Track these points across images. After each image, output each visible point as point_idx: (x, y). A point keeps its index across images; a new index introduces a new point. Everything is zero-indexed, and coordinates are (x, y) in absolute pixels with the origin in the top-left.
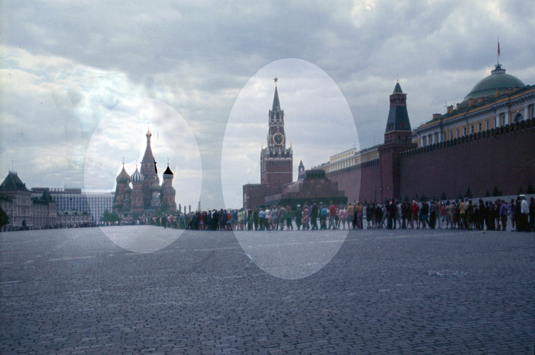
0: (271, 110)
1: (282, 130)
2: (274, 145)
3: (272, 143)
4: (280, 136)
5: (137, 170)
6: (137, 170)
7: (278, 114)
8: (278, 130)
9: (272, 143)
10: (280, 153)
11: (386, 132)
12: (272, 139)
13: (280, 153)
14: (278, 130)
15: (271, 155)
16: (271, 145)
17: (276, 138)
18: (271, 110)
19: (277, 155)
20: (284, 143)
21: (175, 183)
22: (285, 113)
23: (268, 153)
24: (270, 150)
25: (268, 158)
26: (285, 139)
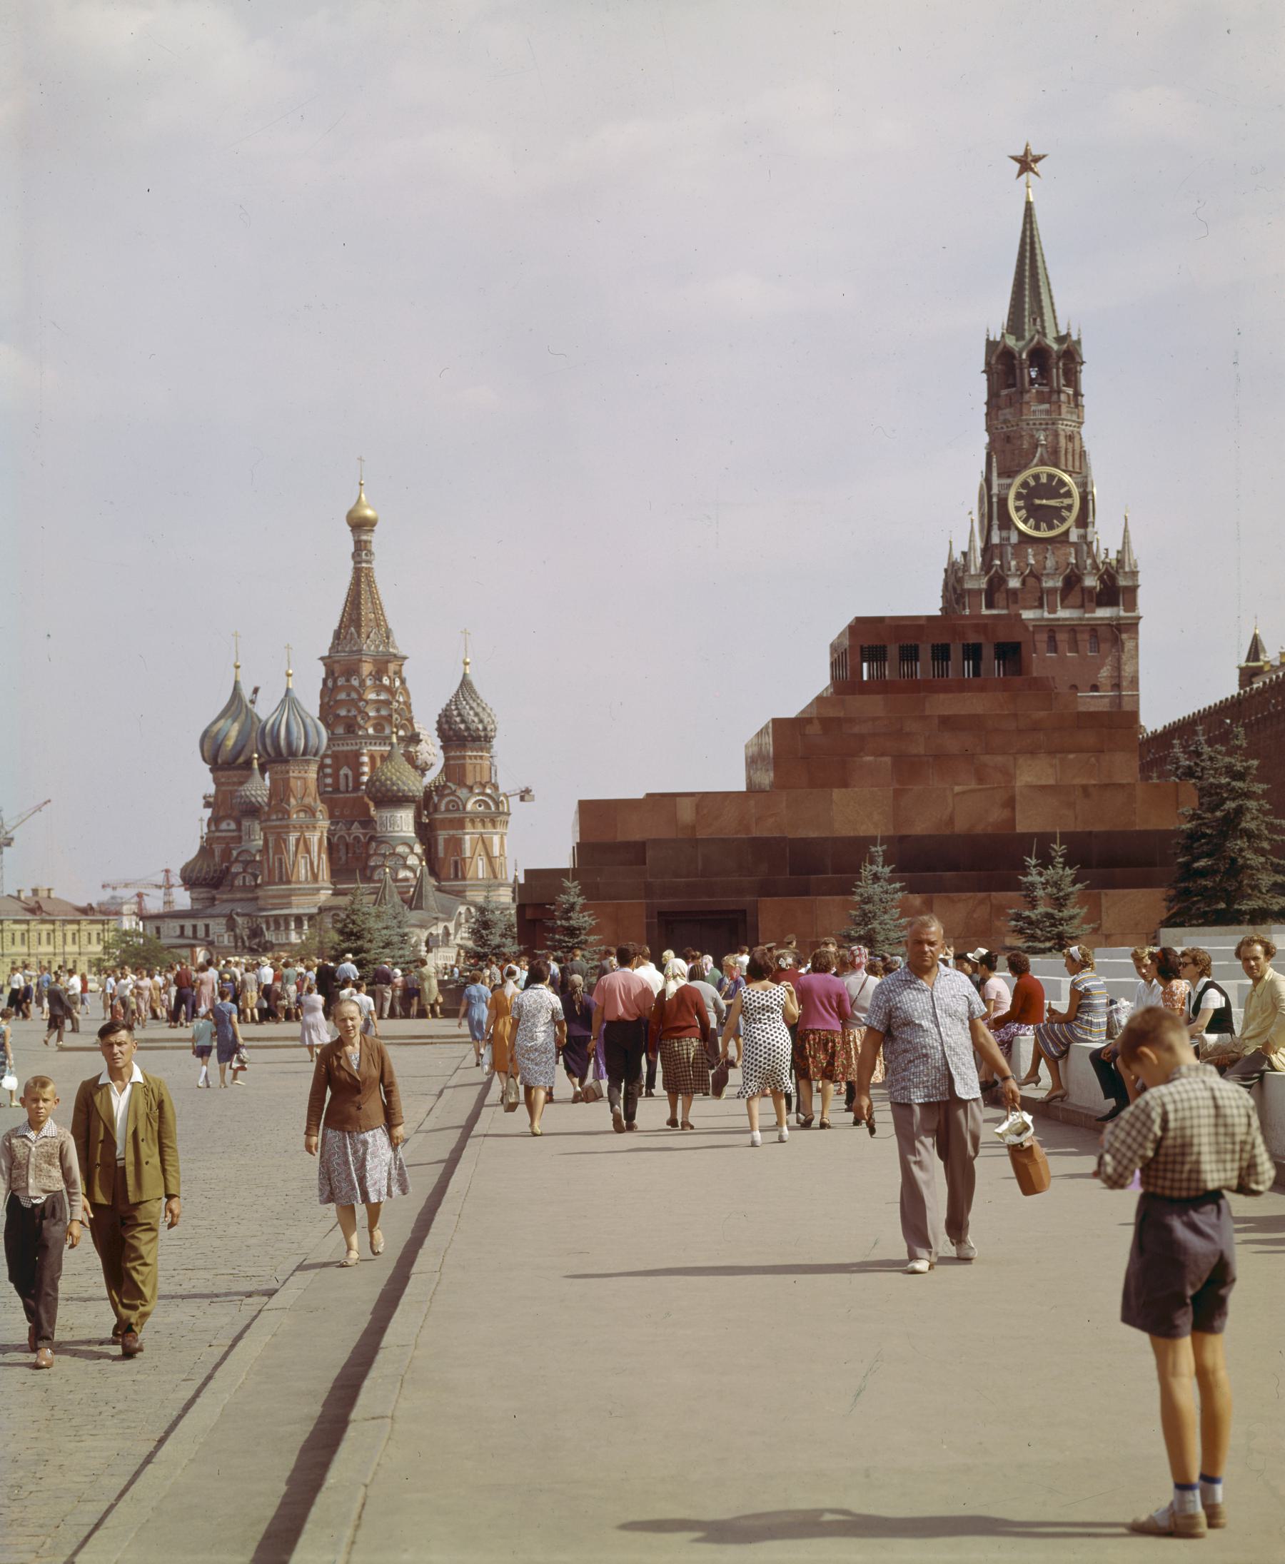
2: (1014, 538)
3: (1006, 523)
4: (1054, 488)
7: (1039, 355)
12: (1003, 502)
17: (1029, 495)
20: (1083, 520)
22: (1086, 352)
26: (1085, 498)
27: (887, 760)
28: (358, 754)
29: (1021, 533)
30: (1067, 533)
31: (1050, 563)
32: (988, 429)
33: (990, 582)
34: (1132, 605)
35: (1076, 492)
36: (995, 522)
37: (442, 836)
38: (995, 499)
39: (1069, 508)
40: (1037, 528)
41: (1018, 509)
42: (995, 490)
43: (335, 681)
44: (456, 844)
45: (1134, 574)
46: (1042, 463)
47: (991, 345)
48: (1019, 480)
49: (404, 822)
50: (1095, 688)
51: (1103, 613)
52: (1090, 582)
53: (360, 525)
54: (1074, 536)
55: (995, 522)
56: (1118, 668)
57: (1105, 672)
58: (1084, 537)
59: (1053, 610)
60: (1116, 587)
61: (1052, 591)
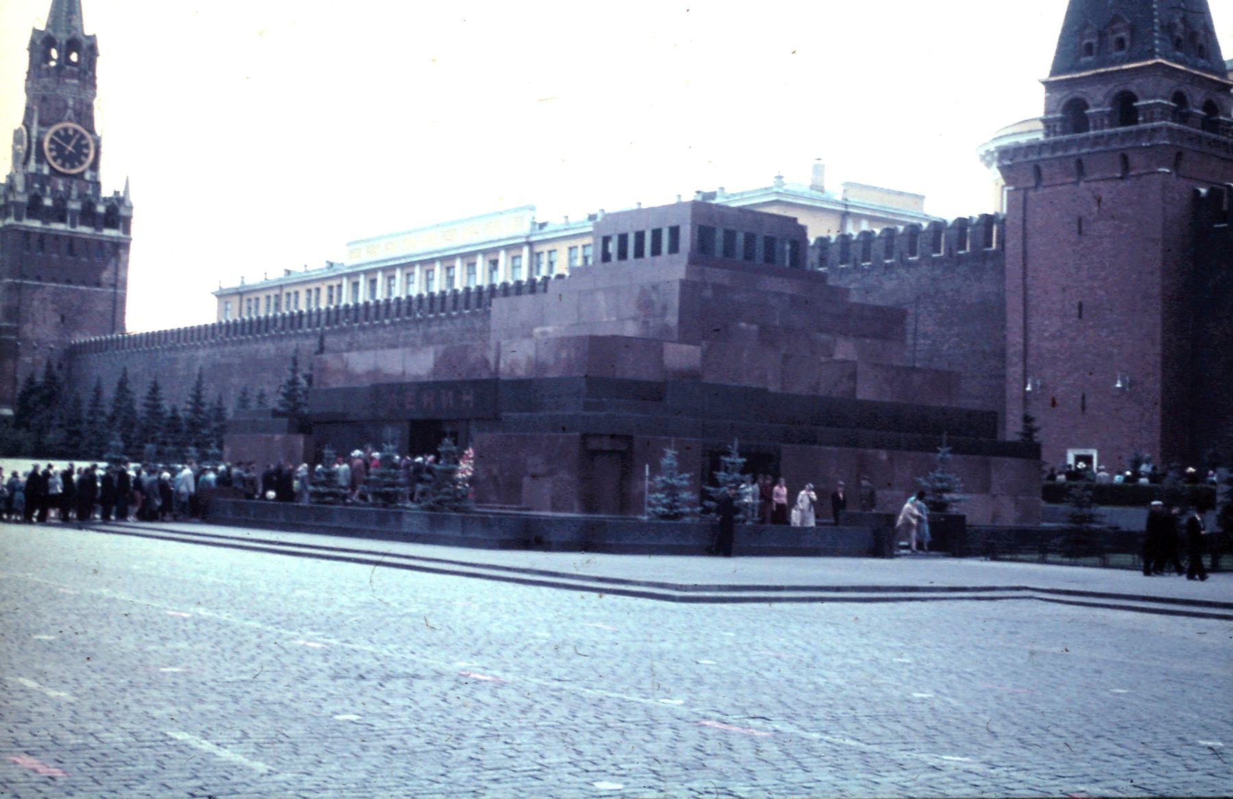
0: (42, 27)
1: (85, 115)
2: (46, 171)
3: (41, 158)
7: (73, 44)
8: (70, 112)
9: (41, 158)
11: (1053, 73)
12: (40, 144)
13: (75, 206)
14: (70, 112)
15: (34, 208)
16: (32, 166)
19: (59, 213)
20: (95, 166)
24: (28, 186)
25: (19, 218)
27: (754, 327)
29: (52, 168)
30: (82, 173)
31: (74, 193)
34: (127, 230)
35: (92, 146)
36: (33, 157)
38: (34, 140)
39: (87, 155)
40: (63, 165)
41: (51, 150)
42: (34, 133)
45: (131, 208)
46: (70, 120)
47: (35, 31)
48: (52, 130)
50: (98, 284)
51: (108, 232)
54: (88, 176)
55: (33, 157)
56: (116, 274)
57: (106, 275)
58: (95, 177)
59: (73, 225)
60: (116, 214)
61: (73, 212)
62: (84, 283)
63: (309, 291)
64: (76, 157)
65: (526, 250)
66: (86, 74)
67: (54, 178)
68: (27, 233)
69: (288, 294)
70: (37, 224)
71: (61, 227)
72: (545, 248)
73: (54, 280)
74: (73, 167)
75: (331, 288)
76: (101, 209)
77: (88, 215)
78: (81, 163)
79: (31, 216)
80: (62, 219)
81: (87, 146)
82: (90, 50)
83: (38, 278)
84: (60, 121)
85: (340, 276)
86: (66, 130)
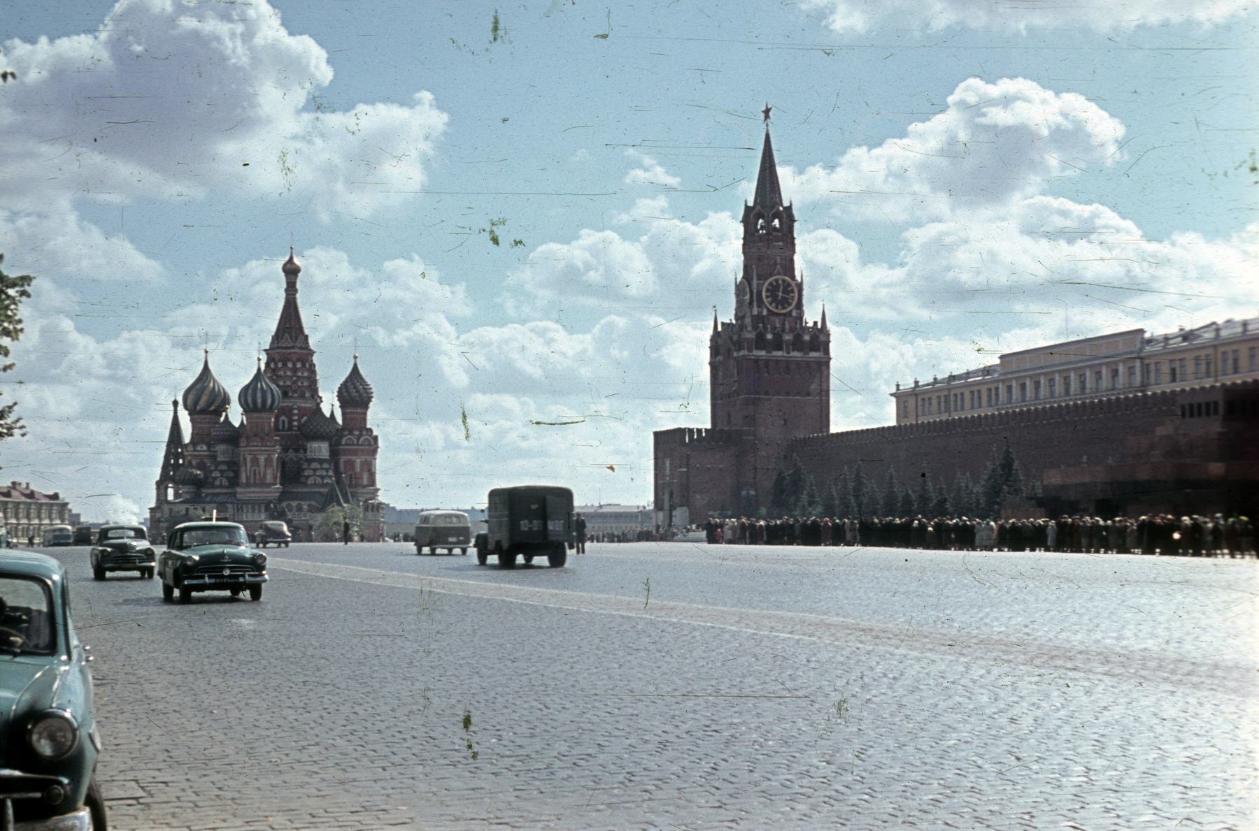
2: (765, 313)
5: (259, 369)
6: (259, 369)
10: (788, 337)
12: (759, 293)
13: (788, 337)
15: (760, 342)
17: (773, 290)
18: (751, 204)
21: (375, 416)
23: (750, 335)
24: (755, 327)
25: (750, 350)
28: (291, 409)
29: (769, 310)
31: (787, 326)
32: (744, 252)
33: (757, 336)
35: (796, 290)
36: (755, 304)
37: (343, 459)
43: (276, 364)
44: (351, 464)
46: (779, 274)
47: (747, 208)
49: (321, 449)
50: (808, 394)
52: (807, 338)
53: (291, 271)
54: (794, 314)
55: (755, 304)
62: (798, 394)
63: (972, 392)
64: (785, 302)
65: (1138, 363)
66: (786, 238)
67: (772, 318)
68: (757, 360)
69: (956, 395)
70: (763, 353)
71: (779, 353)
72: (1153, 361)
73: (778, 394)
74: (784, 308)
75: (990, 390)
76: (807, 338)
77: (798, 344)
78: (790, 304)
79: (757, 348)
80: (779, 348)
81: (792, 291)
82: (788, 217)
83: (767, 393)
84: (771, 275)
85: (998, 381)
86: (777, 281)
